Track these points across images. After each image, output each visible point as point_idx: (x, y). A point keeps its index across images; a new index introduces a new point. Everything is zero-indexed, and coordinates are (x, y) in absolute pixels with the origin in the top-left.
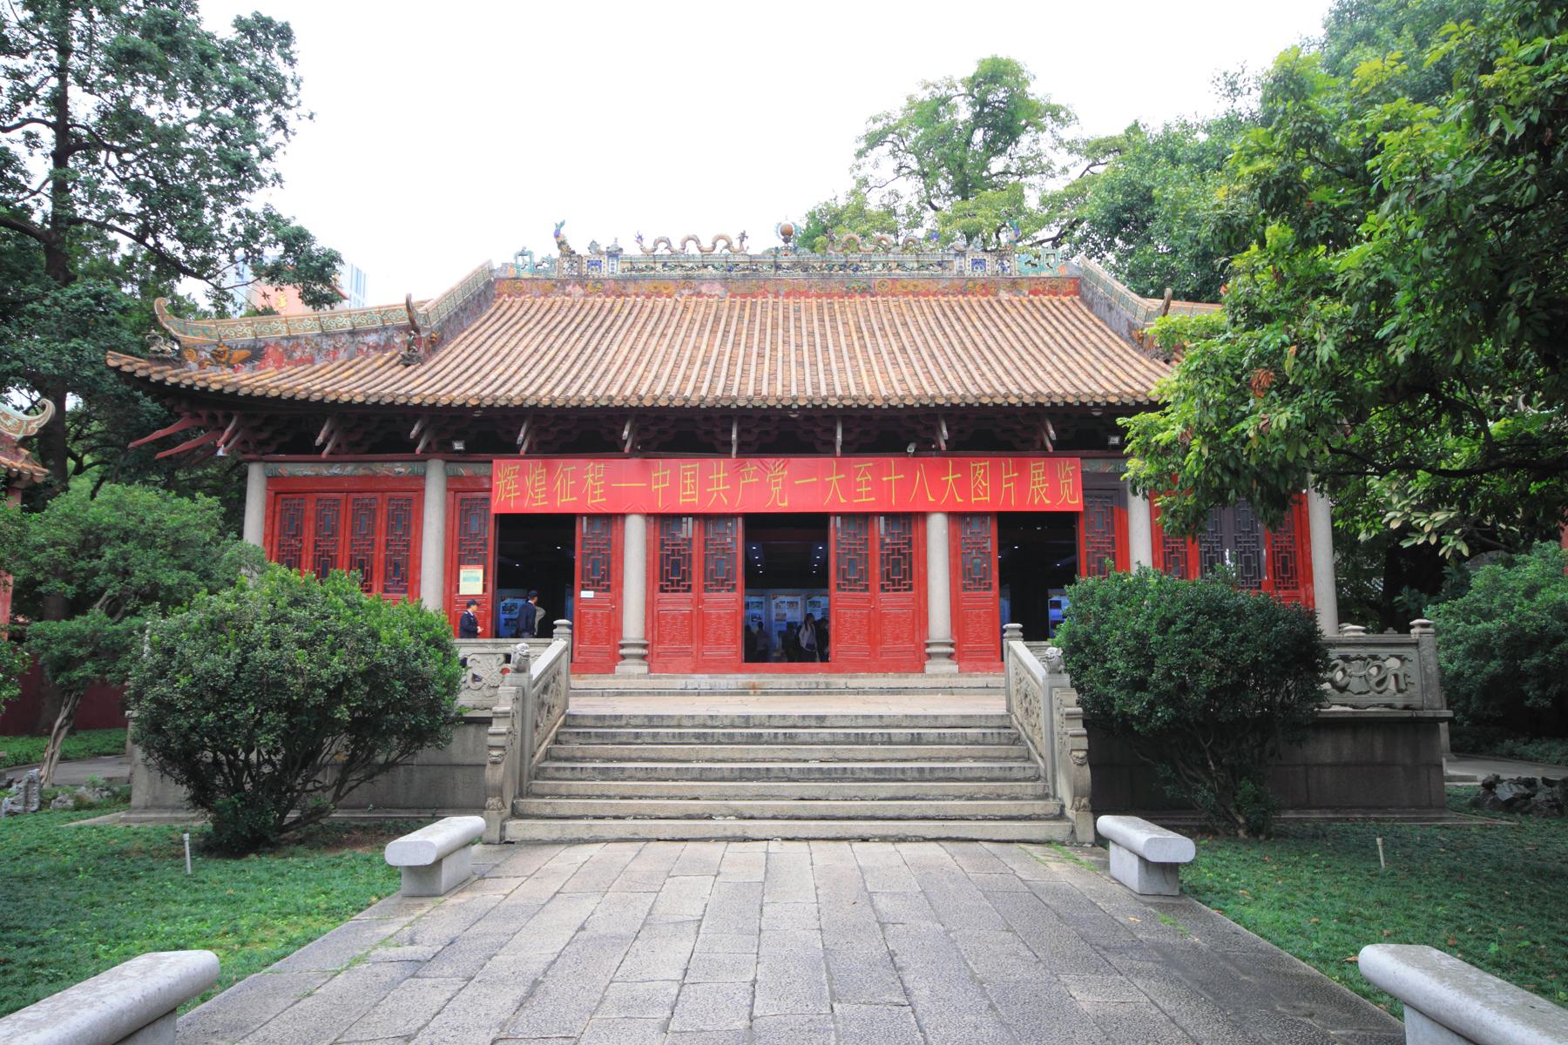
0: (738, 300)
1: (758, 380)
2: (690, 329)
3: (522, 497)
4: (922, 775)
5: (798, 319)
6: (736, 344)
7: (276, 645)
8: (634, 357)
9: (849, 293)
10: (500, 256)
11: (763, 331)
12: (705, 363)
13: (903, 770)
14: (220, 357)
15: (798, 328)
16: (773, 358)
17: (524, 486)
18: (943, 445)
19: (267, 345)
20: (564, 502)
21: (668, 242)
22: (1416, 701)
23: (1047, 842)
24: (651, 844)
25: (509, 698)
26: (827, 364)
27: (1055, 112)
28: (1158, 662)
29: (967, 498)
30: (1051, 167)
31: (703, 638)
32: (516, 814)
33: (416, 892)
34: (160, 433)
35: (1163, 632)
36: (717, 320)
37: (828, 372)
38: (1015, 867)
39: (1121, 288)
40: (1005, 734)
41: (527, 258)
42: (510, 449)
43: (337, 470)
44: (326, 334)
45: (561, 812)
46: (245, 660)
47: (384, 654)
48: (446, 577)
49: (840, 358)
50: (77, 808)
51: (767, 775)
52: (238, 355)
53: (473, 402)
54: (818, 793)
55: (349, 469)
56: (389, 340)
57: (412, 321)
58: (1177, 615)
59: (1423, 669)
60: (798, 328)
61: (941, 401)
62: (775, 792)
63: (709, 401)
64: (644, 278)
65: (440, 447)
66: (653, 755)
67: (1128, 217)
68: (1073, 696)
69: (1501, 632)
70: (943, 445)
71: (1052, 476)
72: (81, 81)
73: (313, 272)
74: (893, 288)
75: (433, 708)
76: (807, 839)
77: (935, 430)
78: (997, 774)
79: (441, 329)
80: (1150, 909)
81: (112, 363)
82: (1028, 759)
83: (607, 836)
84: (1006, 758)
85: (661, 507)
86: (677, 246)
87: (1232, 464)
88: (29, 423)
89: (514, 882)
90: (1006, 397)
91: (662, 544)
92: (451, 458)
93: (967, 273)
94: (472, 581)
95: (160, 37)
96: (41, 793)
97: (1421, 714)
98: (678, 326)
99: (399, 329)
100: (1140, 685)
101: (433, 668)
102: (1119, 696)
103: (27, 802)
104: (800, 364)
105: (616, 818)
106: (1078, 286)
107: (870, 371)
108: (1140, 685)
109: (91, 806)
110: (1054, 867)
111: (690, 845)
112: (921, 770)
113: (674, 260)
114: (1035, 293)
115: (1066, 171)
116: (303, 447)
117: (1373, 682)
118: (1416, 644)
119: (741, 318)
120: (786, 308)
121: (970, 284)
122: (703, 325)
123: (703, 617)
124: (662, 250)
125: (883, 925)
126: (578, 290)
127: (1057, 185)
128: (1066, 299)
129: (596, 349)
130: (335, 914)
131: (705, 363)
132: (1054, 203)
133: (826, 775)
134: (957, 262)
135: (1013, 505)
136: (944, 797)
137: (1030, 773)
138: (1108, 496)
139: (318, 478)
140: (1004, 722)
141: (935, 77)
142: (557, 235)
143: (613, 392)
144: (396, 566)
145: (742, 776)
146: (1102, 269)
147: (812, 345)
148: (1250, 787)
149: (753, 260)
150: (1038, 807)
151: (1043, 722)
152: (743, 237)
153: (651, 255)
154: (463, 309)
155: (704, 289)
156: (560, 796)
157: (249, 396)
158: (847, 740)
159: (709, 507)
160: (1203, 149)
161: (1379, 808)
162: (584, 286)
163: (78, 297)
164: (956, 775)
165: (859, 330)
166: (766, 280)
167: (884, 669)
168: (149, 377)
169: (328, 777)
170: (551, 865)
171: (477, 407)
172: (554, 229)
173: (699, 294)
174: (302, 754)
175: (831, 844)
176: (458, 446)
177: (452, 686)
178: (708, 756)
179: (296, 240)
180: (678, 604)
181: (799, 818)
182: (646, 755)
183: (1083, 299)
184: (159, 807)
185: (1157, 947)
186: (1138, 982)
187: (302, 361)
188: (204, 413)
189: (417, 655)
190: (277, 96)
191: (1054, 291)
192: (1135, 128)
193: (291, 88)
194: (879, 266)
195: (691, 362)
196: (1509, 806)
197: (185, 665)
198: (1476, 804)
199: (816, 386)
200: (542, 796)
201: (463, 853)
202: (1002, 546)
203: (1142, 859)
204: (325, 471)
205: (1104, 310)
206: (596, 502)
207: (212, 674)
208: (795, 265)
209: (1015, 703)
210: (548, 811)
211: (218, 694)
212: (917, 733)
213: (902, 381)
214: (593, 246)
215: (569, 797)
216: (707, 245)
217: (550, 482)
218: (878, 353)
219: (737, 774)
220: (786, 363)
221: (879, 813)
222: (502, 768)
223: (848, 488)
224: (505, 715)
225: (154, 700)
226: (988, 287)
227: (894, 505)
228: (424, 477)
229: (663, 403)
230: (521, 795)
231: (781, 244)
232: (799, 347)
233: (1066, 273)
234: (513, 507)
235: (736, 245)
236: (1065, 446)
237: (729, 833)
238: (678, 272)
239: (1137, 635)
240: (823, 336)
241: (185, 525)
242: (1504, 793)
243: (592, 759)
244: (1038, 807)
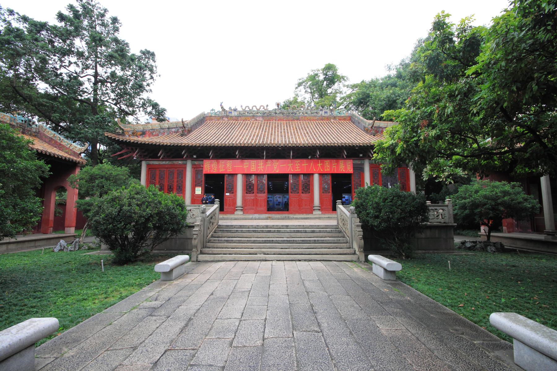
0: (266, 122)
1: (271, 140)
3: (211, 170)
4: (315, 242)
5: (281, 126)
6: (265, 132)
7: (130, 205)
9: (294, 120)
10: (207, 110)
11: (272, 129)
12: (257, 136)
13: (310, 240)
14: (134, 134)
15: (281, 128)
16: (275, 135)
17: (212, 166)
20: (221, 171)
22: (447, 221)
23: (351, 261)
24: (239, 262)
26: (288, 136)
27: (343, 78)
28: (383, 211)
29: (323, 169)
30: (342, 90)
31: (257, 205)
32: (202, 253)
34: (119, 153)
35: (384, 202)
36: (261, 126)
37: (289, 138)
38: (344, 270)
39: (362, 118)
40: (337, 230)
42: (208, 157)
43: (164, 163)
44: (161, 128)
45: (214, 252)
46: (121, 210)
47: (163, 208)
48: (192, 189)
49: (291, 135)
50: (89, 249)
51: (272, 242)
52: (139, 133)
53: (198, 145)
54: (286, 247)
55: (167, 162)
56: (178, 130)
58: (388, 197)
59: (449, 212)
60: (281, 128)
63: (258, 145)
65: (190, 157)
67: (362, 101)
68: (358, 220)
69: (469, 203)
71: (345, 164)
72: (100, 65)
73: (159, 114)
74: (305, 119)
75: (178, 224)
76: (283, 261)
77: (316, 152)
78: (336, 241)
79: (191, 128)
80: (389, 285)
81: (106, 135)
82: (344, 237)
83: (227, 259)
84: (338, 237)
85: (246, 172)
86: (251, 108)
87: (412, 150)
89: (197, 275)
91: (247, 182)
92: (193, 160)
94: (199, 191)
95: (119, 52)
96: (79, 245)
97: (448, 224)
98: (251, 127)
100: (377, 217)
101: (178, 212)
102: (371, 220)
103: (75, 247)
104: (281, 136)
105: (230, 254)
106: (351, 119)
107: (299, 138)
108: (377, 217)
109: (92, 249)
110: (356, 270)
111: (250, 262)
112: (315, 240)
113: (250, 112)
114: (340, 120)
117: (436, 216)
118: (447, 206)
119: (267, 126)
120: (278, 124)
122: (257, 127)
123: (257, 200)
124: (247, 109)
125: (307, 292)
126: (226, 119)
130: (140, 286)
131: (257, 136)
132: (344, 99)
133: (289, 242)
134: (320, 112)
135: (335, 172)
136: (321, 248)
137: (345, 241)
138: (359, 169)
139: (159, 165)
140: (337, 227)
141: (315, 68)
142: (221, 105)
143: (234, 142)
144: (179, 187)
145: (265, 242)
146: (356, 113)
147: (285, 132)
149: (270, 111)
150: (348, 251)
151: (349, 227)
152: (267, 106)
153: (244, 110)
154: (197, 123)
156: (215, 248)
157: (141, 143)
158: (294, 232)
159: (258, 172)
160: (382, 84)
161: (437, 250)
162: (228, 118)
163: (98, 118)
164: (325, 242)
165: (296, 128)
167: (302, 213)
169: (149, 242)
170: (209, 269)
171: (199, 146)
173: (256, 120)
174: (140, 236)
175: (290, 262)
176: (195, 157)
177: (184, 217)
179: (155, 106)
180: (250, 197)
181: (281, 254)
183: (352, 121)
185: (398, 302)
187: (155, 135)
188: (130, 148)
189: (174, 208)
190: (151, 70)
191: (345, 119)
192: (363, 81)
193: (154, 68)
195: (254, 136)
196: (470, 249)
197: (104, 211)
198: (460, 248)
200: (210, 248)
201: (181, 267)
202: (333, 182)
203: (385, 270)
204: (161, 163)
205: (357, 123)
206: (230, 171)
207: (111, 214)
208: (280, 113)
209: (340, 222)
210: (211, 252)
212: (313, 230)
213: (307, 140)
214: (230, 108)
215: (217, 248)
216: (258, 108)
217: (218, 166)
218: (301, 134)
220: (278, 136)
221: (304, 253)
222: (197, 240)
223: (293, 167)
224: (198, 225)
225: (95, 221)
226: (328, 119)
227: (305, 171)
228: (186, 164)
229: (246, 145)
230: (203, 248)
231: (277, 108)
232: (281, 132)
233: (347, 115)
234: (209, 172)
235: (266, 108)
236: (349, 157)
238: (251, 115)
239: (376, 203)
240: (287, 130)
241: (118, 175)
242: (468, 245)
243: (224, 237)
244: (348, 251)
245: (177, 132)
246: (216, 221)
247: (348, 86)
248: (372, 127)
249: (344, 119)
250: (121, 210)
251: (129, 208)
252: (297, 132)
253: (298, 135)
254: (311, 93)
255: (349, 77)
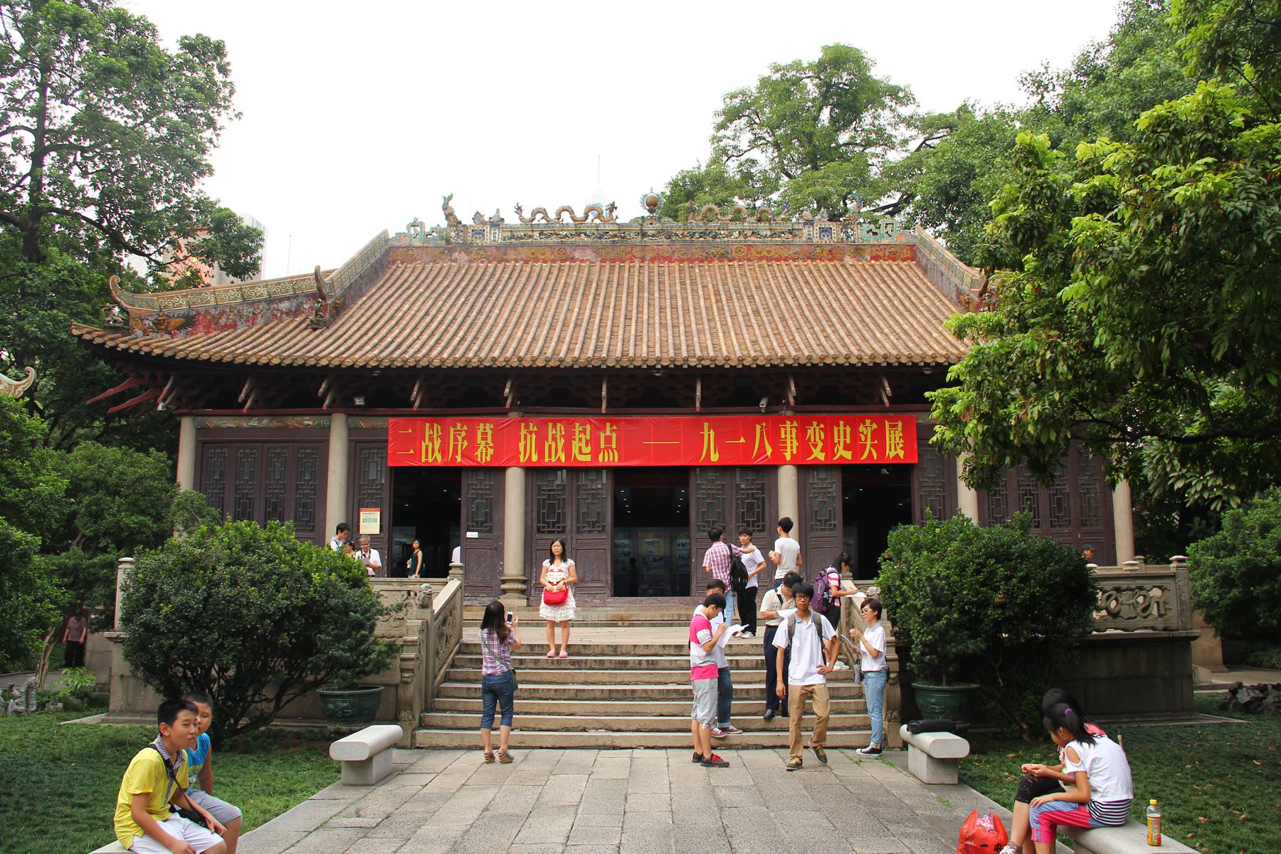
2: (563, 293)
7: (234, 583)
8: (514, 319)
10: (396, 226)
11: (629, 294)
14: (161, 325)
18: (792, 400)
19: (198, 313)
21: (544, 212)
25: (416, 630)
27: (894, 92)
32: (423, 725)
33: (353, 782)
37: (688, 334)
39: (950, 256)
41: (418, 229)
43: (254, 423)
46: (210, 595)
47: (315, 591)
49: (699, 321)
51: (632, 695)
52: (175, 322)
54: (675, 711)
57: (320, 289)
61: (790, 362)
62: (637, 710)
64: (523, 245)
65: (344, 404)
66: (535, 678)
67: (953, 197)
70: (792, 400)
73: (234, 246)
74: (748, 254)
76: (665, 748)
79: (343, 296)
81: (75, 332)
86: (552, 216)
88: (16, 387)
89: (427, 778)
90: (847, 357)
92: (352, 411)
93: (815, 240)
94: (370, 523)
97: (1176, 634)
99: (307, 296)
111: (568, 751)
114: (876, 258)
115: (906, 145)
116: (228, 404)
121: (818, 250)
122: (575, 289)
125: (721, 809)
126: (462, 257)
127: (895, 156)
128: (903, 264)
129: (480, 312)
132: (894, 174)
134: (806, 231)
139: (239, 429)
141: (785, 61)
142: (445, 207)
143: (496, 354)
145: (611, 696)
146: (934, 238)
148: (1032, 697)
149: (622, 229)
155: (577, 255)
157: (184, 359)
165: (717, 293)
166: (634, 246)
168: (104, 344)
172: (442, 201)
173: (573, 260)
176: (359, 402)
178: (582, 680)
182: (529, 678)
183: (919, 264)
184: (131, 711)
186: (906, 841)
187: (226, 327)
192: (963, 109)
194: (736, 234)
195: (565, 325)
197: (165, 598)
199: (677, 348)
200: (444, 711)
207: (186, 606)
208: (659, 232)
210: (449, 723)
211: (191, 622)
213: (755, 342)
214: (477, 216)
218: (734, 316)
219: (606, 695)
224: (413, 643)
225: (144, 625)
228: (328, 429)
229: (540, 363)
230: (427, 710)
231: (646, 214)
233: (904, 240)
235: (605, 214)
237: (600, 743)
240: (685, 299)
242: (1243, 697)
245: (296, 312)
246: (456, 633)
247: (909, 122)
248: (981, 295)
249: (892, 254)
250: (210, 595)
251: (235, 591)
252: (721, 309)
253: (724, 324)
254: (777, 146)
255: (914, 90)
